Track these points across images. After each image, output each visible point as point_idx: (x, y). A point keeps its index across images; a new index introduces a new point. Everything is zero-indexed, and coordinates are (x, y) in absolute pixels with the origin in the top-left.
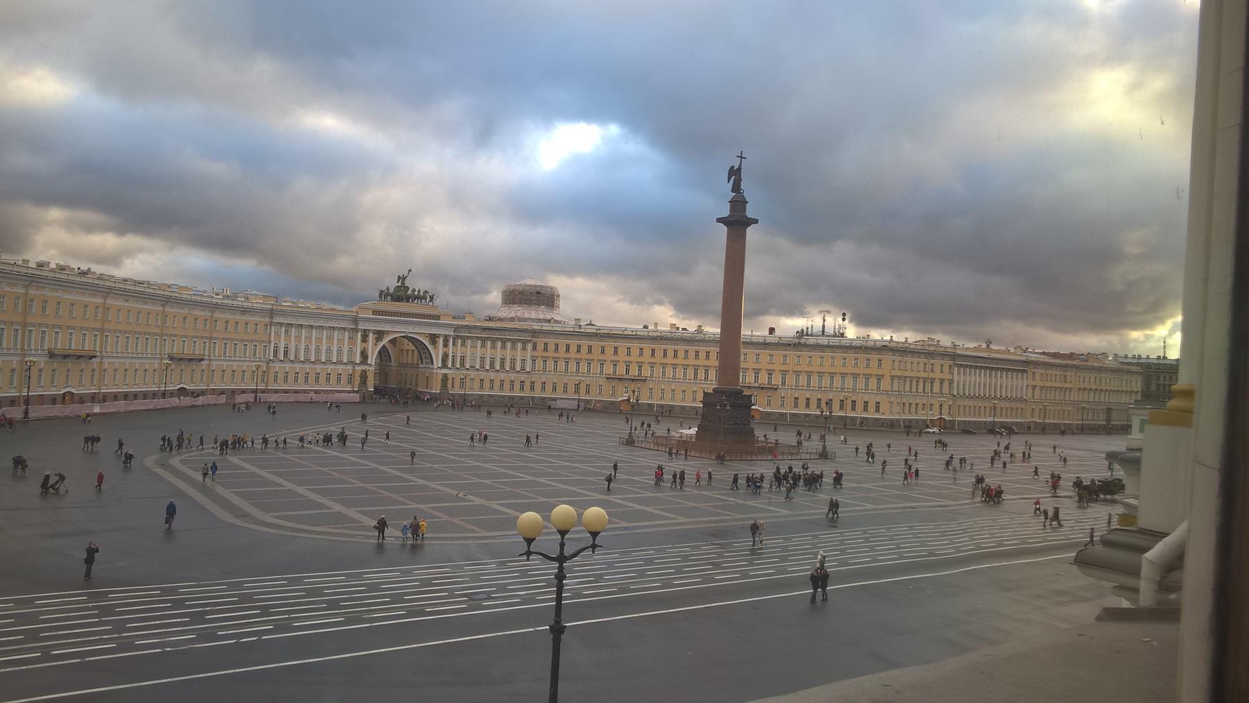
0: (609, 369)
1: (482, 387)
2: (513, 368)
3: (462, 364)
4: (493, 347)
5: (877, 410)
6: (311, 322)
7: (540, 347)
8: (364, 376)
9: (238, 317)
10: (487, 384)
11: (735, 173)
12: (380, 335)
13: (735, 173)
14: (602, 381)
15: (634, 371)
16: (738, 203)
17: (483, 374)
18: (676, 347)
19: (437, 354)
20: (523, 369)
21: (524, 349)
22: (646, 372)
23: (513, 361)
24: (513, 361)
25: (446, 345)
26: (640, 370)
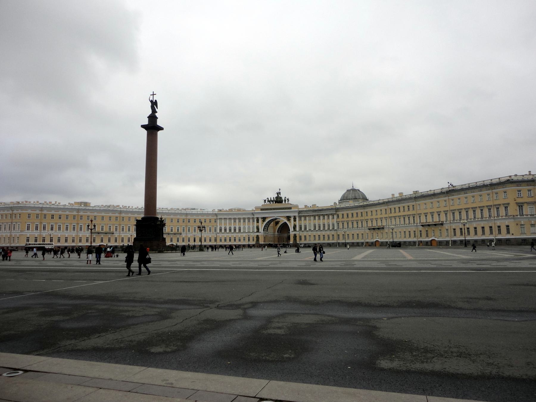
0: (370, 225)
1: (315, 239)
2: (329, 229)
3: (305, 228)
4: (319, 219)
5: (508, 232)
7: (341, 216)
8: (258, 237)
10: (317, 238)
11: (154, 104)
12: (264, 219)
13: (154, 104)
14: (368, 231)
15: (380, 224)
16: (153, 118)
17: (314, 233)
19: (291, 225)
20: (333, 228)
22: (384, 224)
23: (329, 226)
24: (329, 226)
25: (295, 220)
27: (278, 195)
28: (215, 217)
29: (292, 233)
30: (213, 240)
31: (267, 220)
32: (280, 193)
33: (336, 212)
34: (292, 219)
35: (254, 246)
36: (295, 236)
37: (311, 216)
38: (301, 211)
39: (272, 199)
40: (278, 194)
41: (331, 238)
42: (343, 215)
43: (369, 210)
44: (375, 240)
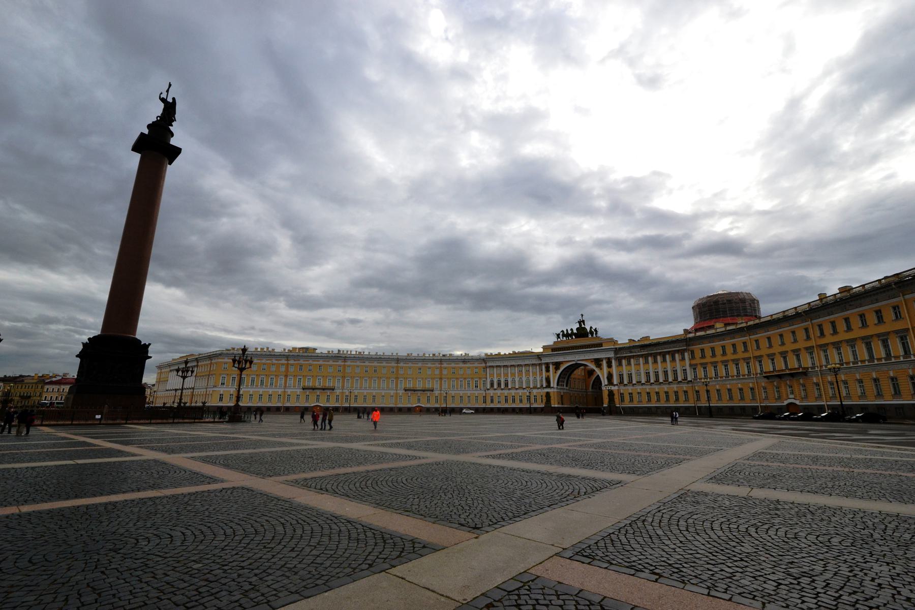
0: (768, 367)
1: (649, 400)
3: (630, 381)
4: (655, 362)
6: (527, 362)
7: (698, 354)
9: (461, 365)
12: (557, 365)
14: (763, 383)
15: (793, 363)
17: (648, 388)
18: (832, 317)
21: (683, 359)
22: (807, 362)
25: (609, 366)
26: (799, 360)
27: (580, 325)
28: (484, 365)
29: (605, 389)
30: (481, 399)
31: (562, 368)
32: (583, 321)
33: (688, 345)
34: (604, 363)
35: (542, 409)
36: (611, 394)
37: (639, 356)
38: (621, 349)
39: (570, 332)
40: (580, 322)
41: (682, 397)
42: (702, 350)
43: (761, 335)
44: (786, 403)
